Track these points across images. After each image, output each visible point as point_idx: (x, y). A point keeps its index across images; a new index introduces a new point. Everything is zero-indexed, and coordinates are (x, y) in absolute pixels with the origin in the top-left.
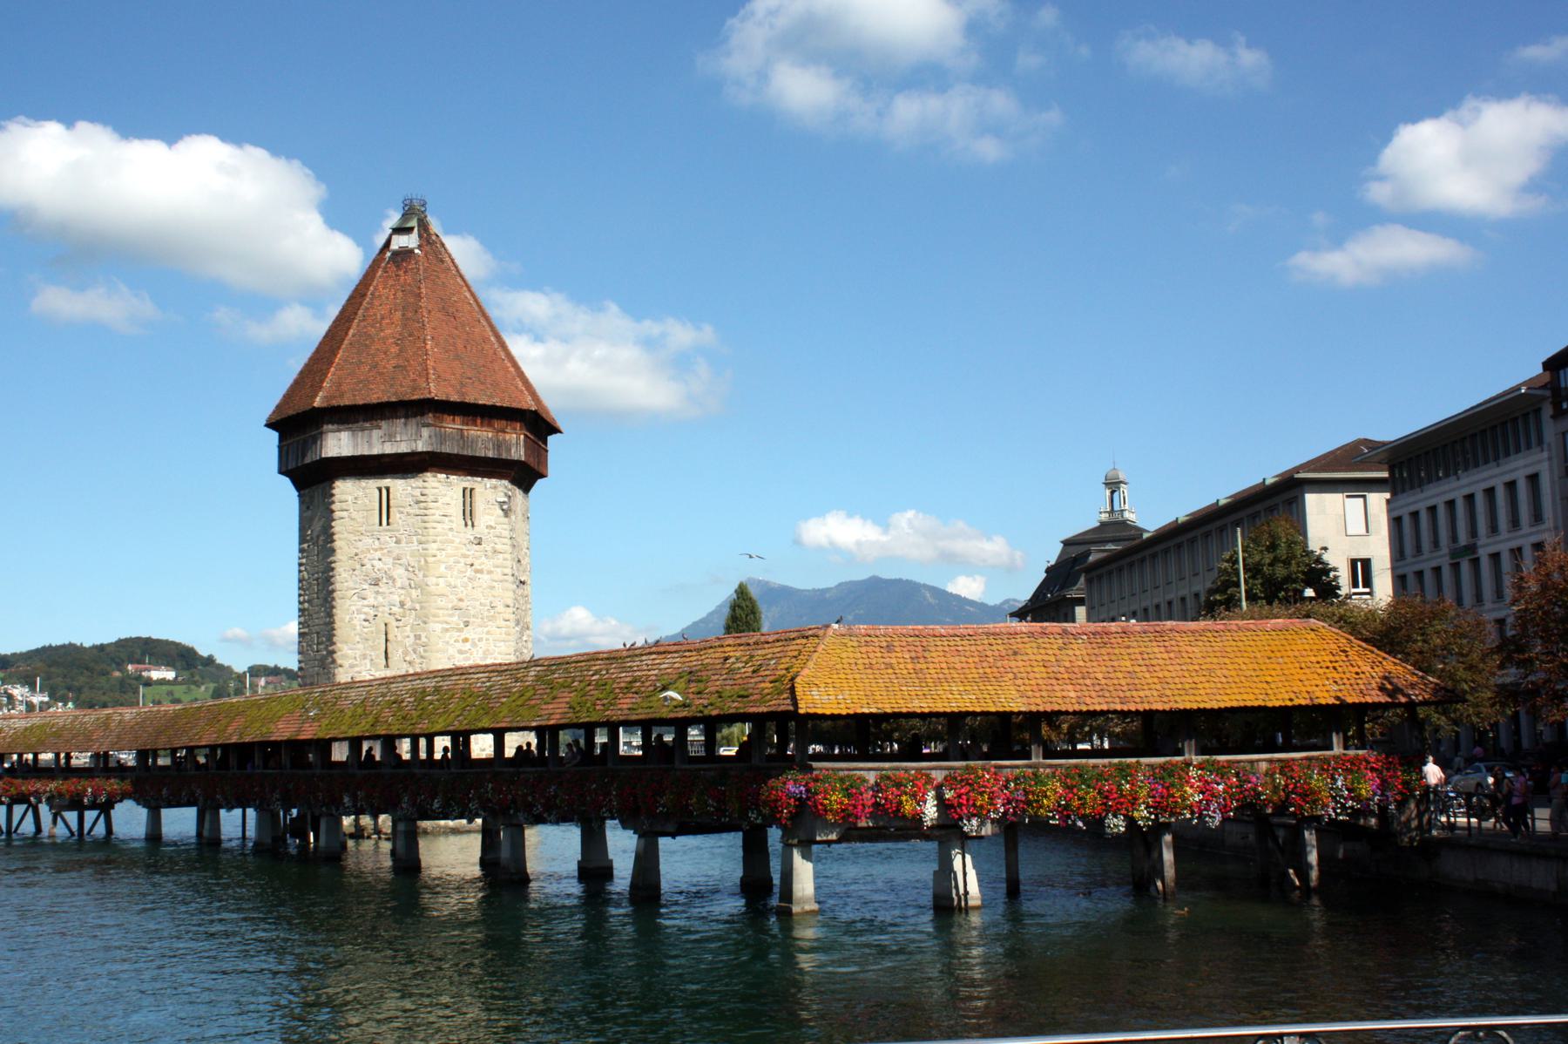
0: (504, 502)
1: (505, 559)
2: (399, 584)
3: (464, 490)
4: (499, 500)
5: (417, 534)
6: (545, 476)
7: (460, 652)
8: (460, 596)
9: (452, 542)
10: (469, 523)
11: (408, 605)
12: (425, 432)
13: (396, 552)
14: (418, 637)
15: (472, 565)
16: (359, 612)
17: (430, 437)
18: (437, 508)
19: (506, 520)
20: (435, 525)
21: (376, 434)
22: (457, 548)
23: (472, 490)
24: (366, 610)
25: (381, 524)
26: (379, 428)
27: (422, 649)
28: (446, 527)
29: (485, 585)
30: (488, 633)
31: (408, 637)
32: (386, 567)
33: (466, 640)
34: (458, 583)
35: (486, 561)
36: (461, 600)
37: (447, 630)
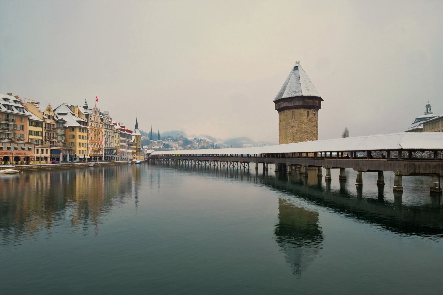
1: (314, 123)
2: (296, 127)
3: (307, 111)
6: (321, 108)
7: (307, 139)
8: (307, 129)
9: (305, 120)
11: (298, 131)
12: (301, 101)
13: (296, 122)
14: (300, 136)
16: (290, 132)
19: (314, 116)
21: (292, 102)
22: (306, 121)
23: (309, 111)
24: (290, 132)
25: (293, 117)
28: (304, 118)
30: (311, 135)
31: (298, 136)
32: (294, 125)
34: (306, 127)
36: (307, 130)
37: (304, 135)
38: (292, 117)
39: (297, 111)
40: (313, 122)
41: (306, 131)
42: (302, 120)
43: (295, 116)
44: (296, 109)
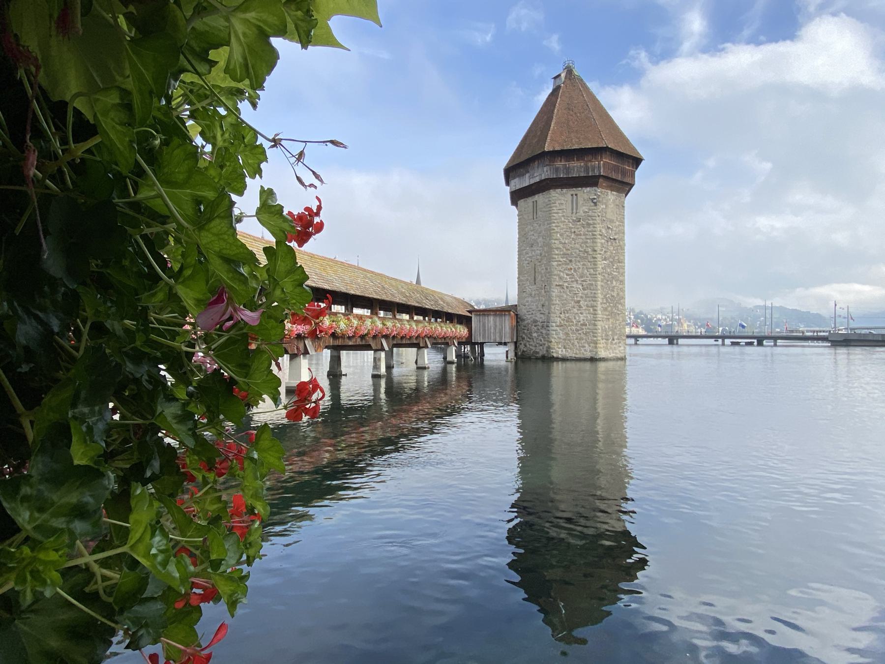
0: (595, 199)
2: (540, 245)
3: (572, 195)
4: (591, 197)
5: (547, 220)
7: (567, 275)
10: (574, 211)
15: (575, 232)
16: (526, 260)
17: (547, 171)
18: (556, 207)
19: (595, 208)
20: (555, 215)
21: (527, 175)
23: (576, 195)
24: (528, 259)
26: (528, 172)
27: (548, 275)
29: (581, 241)
33: (571, 269)
35: (583, 230)
37: (560, 265)
38: (531, 217)
39: (540, 198)
40: (589, 224)
41: (564, 254)
42: (554, 223)
43: (539, 213)
44: (541, 194)
